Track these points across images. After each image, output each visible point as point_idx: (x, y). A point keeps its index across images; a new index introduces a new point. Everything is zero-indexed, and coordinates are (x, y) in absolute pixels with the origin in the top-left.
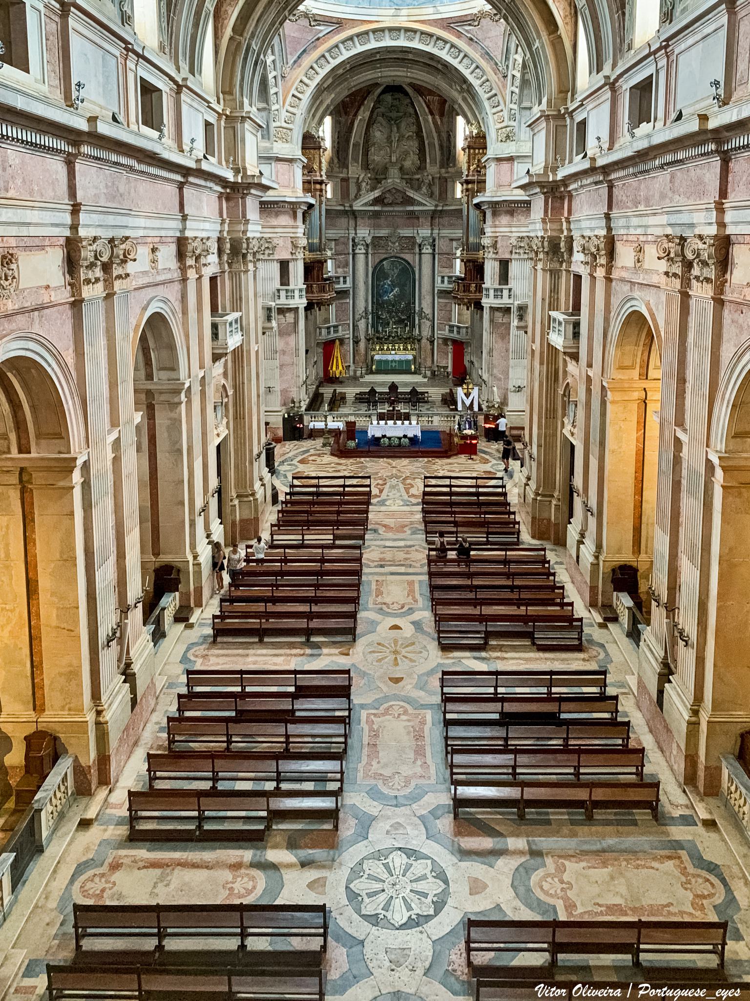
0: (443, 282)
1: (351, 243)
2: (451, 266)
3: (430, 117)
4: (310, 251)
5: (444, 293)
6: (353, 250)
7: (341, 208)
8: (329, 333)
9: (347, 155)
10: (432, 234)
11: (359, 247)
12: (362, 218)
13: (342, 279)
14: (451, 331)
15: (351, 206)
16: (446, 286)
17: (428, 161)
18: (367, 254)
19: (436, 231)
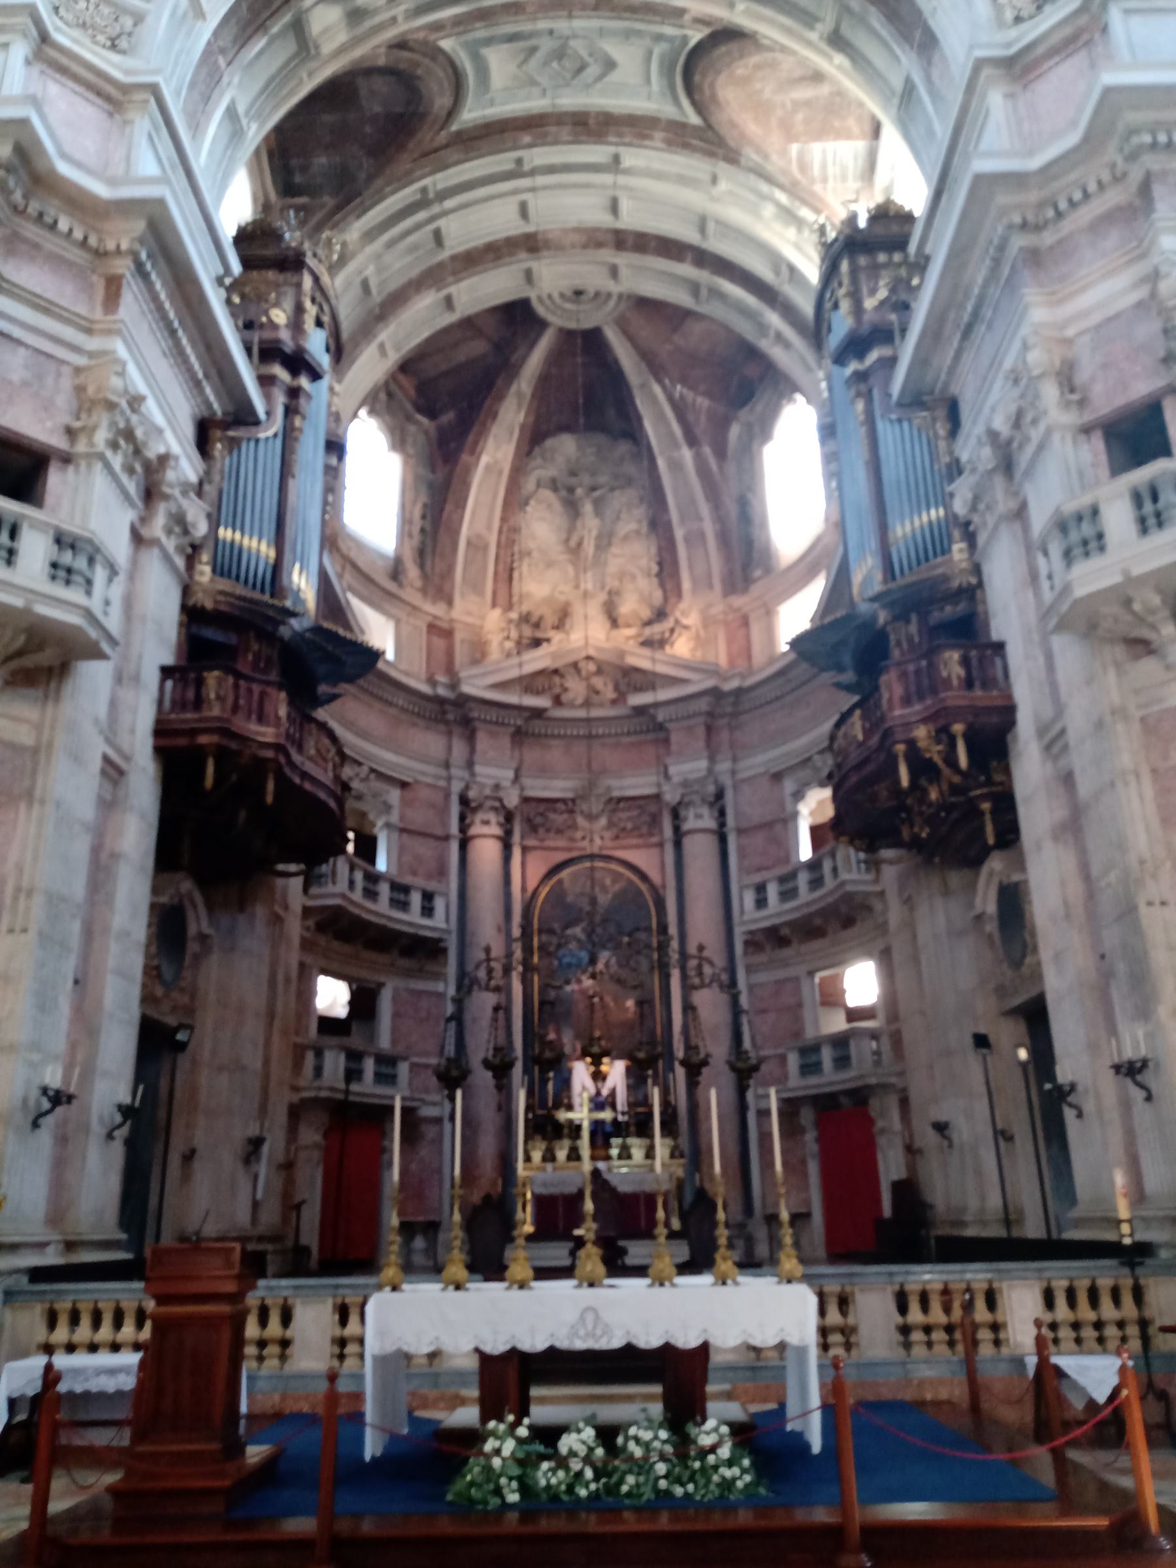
0: (761, 903)
1: (455, 809)
2: (788, 845)
3: (687, 454)
4: (219, 570)
5: (774, 938)
6: (463, 828)
7: (425, 688)
8: (353, 1074)
9: (451, 568)
10: (710, 771)
11: (480, 816)
12: (492, 735)
13: (416, 899)
14: (810, 1068)
15: (454, 685)
16: (776, 910)
17: (686, 585)
18: (507, 847)
19: (723, 766)
